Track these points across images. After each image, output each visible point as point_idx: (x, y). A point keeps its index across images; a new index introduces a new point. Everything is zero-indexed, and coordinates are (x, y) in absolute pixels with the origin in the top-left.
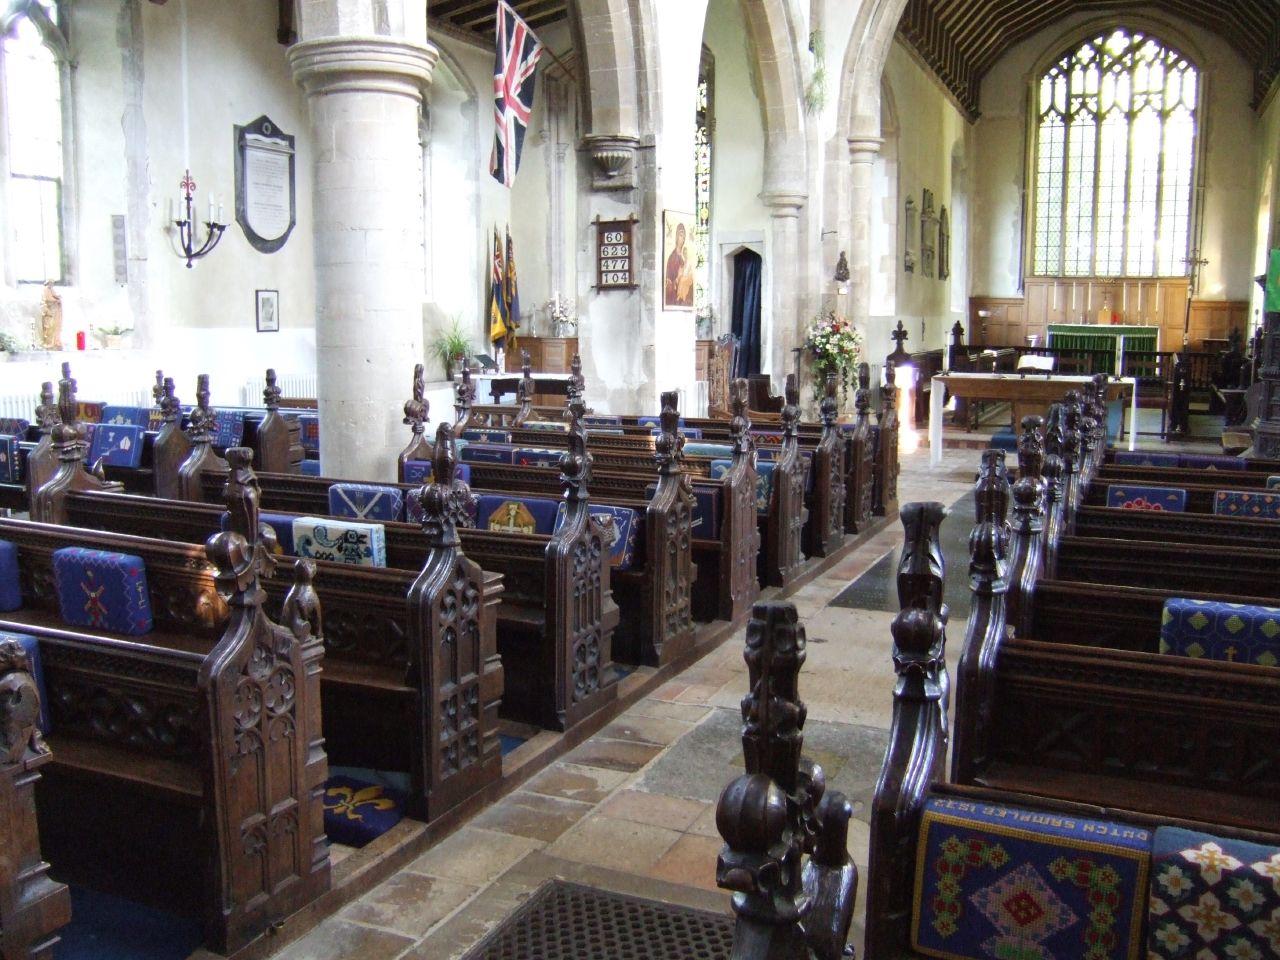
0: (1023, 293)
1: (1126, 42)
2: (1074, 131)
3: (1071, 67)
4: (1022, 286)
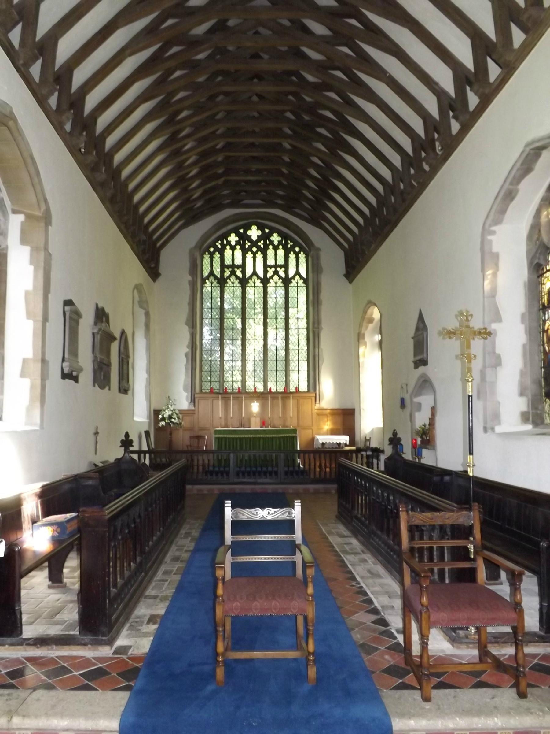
0: (195, 406)
1: (259, 233)
2: (271, 289)
3: (224, 247)
4: (193, 401)
